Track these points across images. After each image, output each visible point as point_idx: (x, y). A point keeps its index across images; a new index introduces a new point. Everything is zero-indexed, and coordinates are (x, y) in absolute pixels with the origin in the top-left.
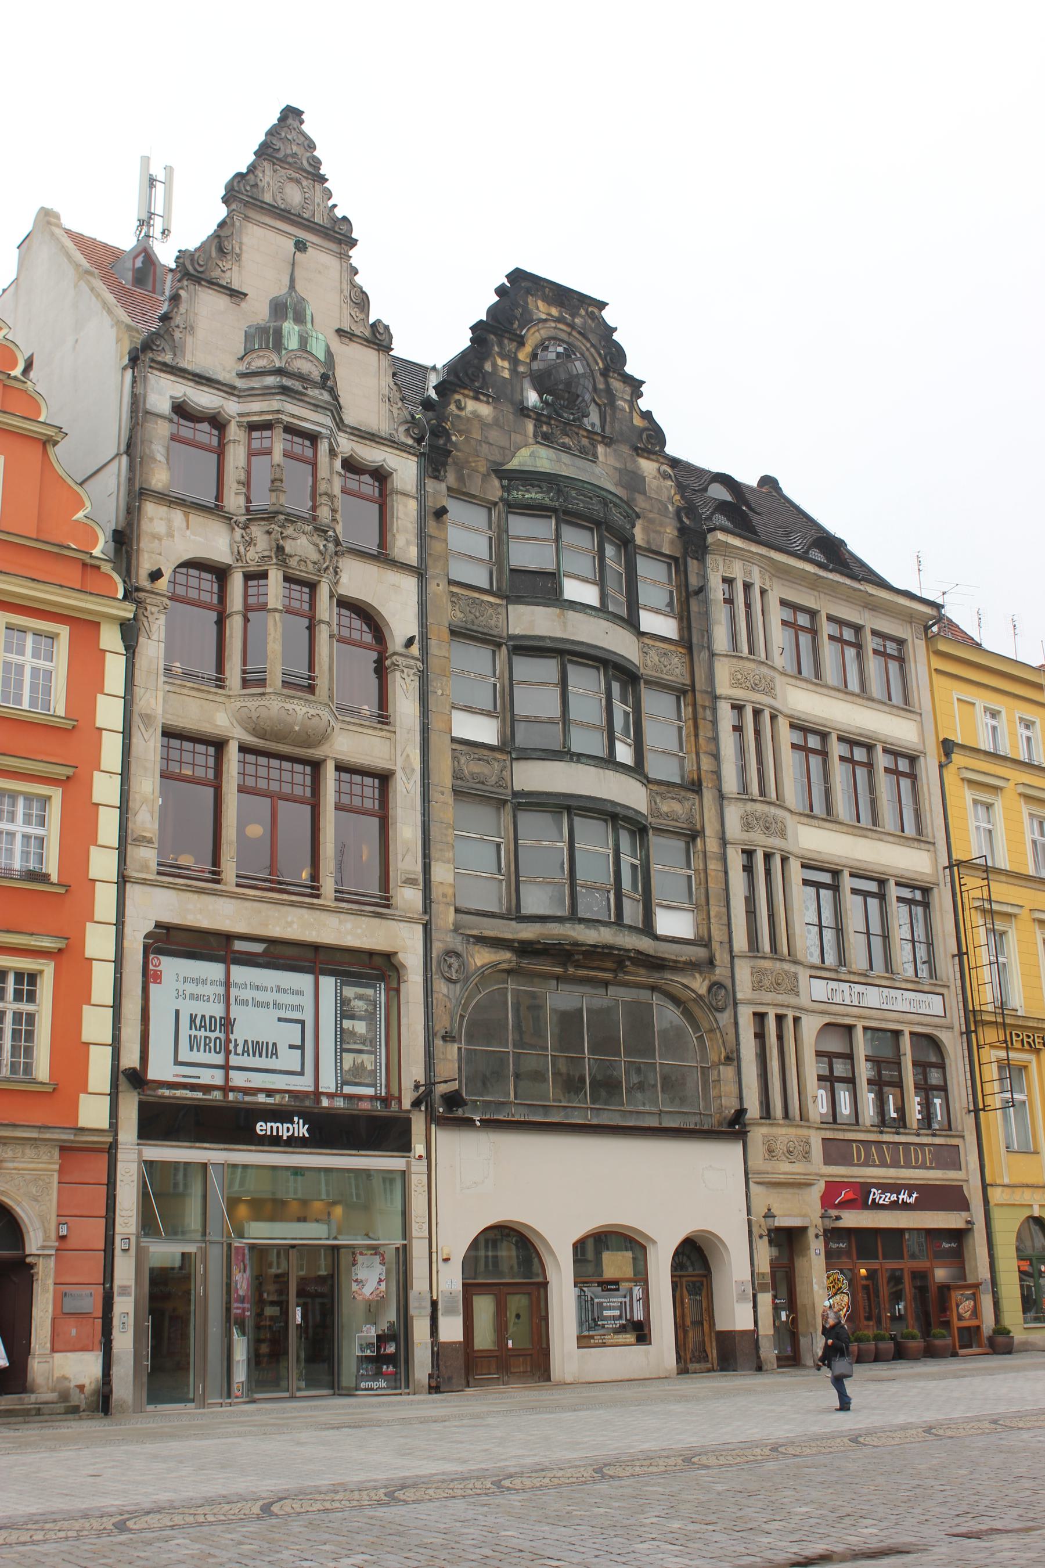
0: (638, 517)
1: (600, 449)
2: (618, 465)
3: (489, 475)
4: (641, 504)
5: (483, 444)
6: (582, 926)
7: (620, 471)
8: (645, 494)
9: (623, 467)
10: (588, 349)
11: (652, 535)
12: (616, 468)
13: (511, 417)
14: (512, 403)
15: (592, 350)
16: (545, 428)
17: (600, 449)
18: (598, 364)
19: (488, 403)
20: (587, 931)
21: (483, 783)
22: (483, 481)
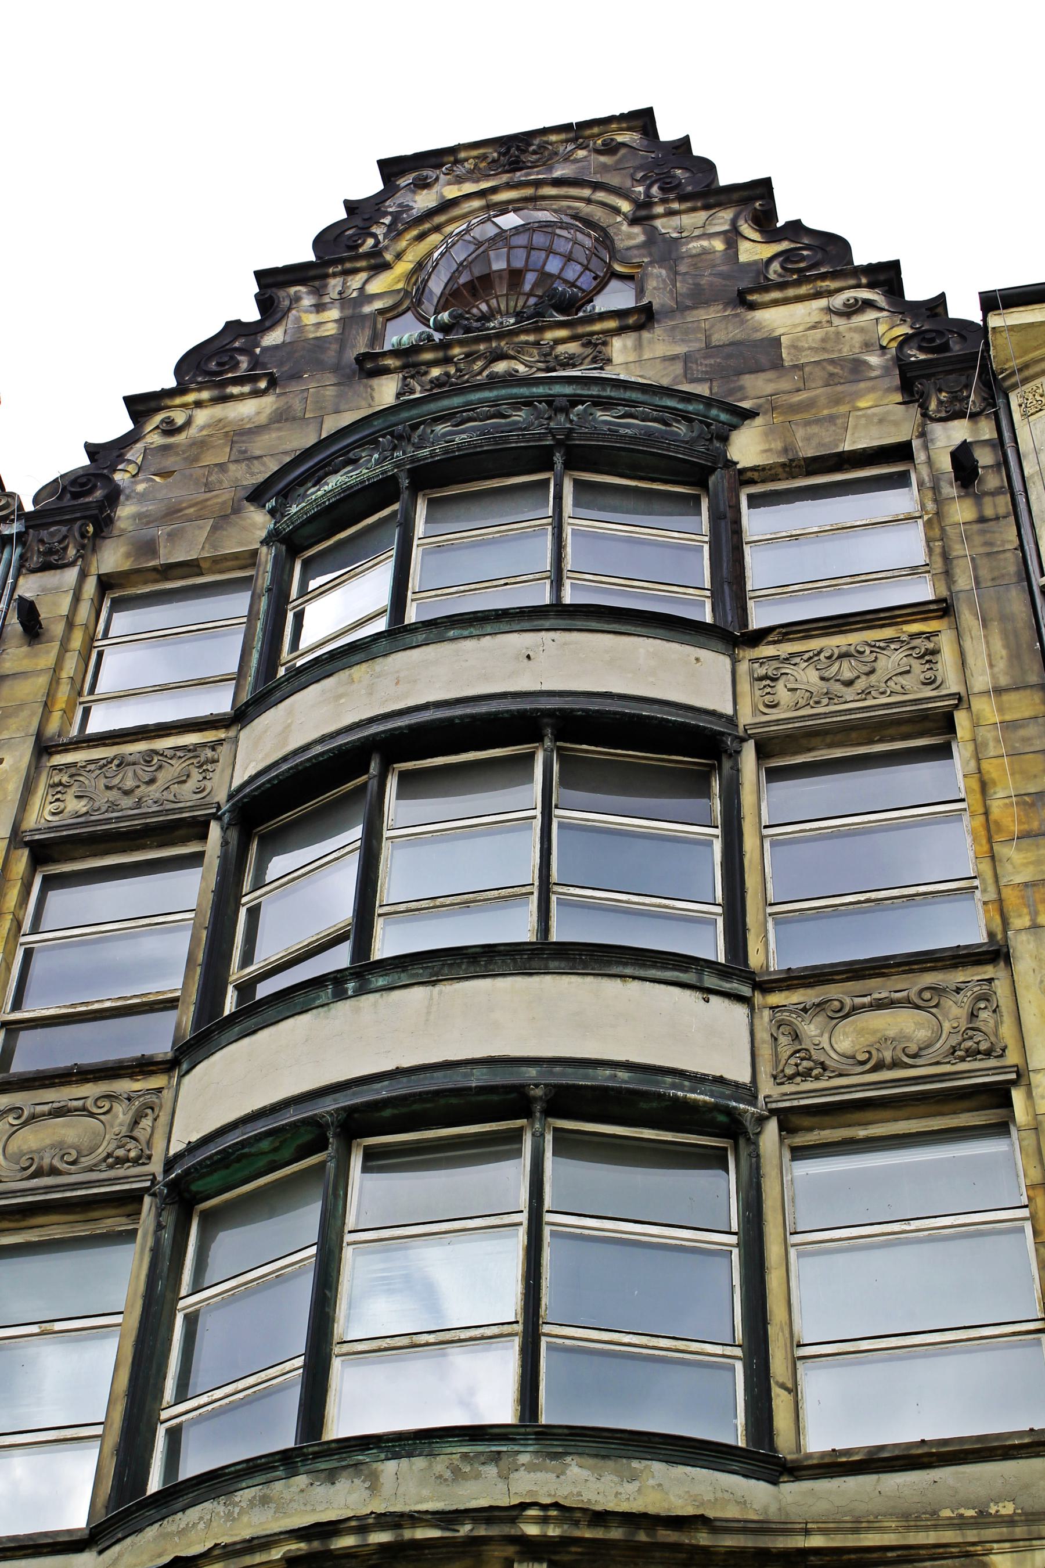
0: (749, 415)
1: (620, 348)
2: (680, 349)
3: (237, 510)
4: (756, 387)
5: (232, 467)
6: (302, 1480)
7: (686, 359)
8: (777, 365)
9: (696, 345)
10: (589, 201)
11: (800, 433)
12: (673, 358)
13: (331, 392)
14: (336, 368)
15: (600, 196)
16: (436, 372)
17: (620, 348)
18: (617, 211)
19: (257, 393)
20: (321, 1491)
21: (54, 1171)
22: (214, 528)
